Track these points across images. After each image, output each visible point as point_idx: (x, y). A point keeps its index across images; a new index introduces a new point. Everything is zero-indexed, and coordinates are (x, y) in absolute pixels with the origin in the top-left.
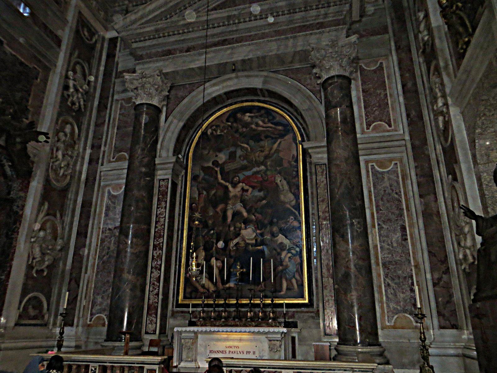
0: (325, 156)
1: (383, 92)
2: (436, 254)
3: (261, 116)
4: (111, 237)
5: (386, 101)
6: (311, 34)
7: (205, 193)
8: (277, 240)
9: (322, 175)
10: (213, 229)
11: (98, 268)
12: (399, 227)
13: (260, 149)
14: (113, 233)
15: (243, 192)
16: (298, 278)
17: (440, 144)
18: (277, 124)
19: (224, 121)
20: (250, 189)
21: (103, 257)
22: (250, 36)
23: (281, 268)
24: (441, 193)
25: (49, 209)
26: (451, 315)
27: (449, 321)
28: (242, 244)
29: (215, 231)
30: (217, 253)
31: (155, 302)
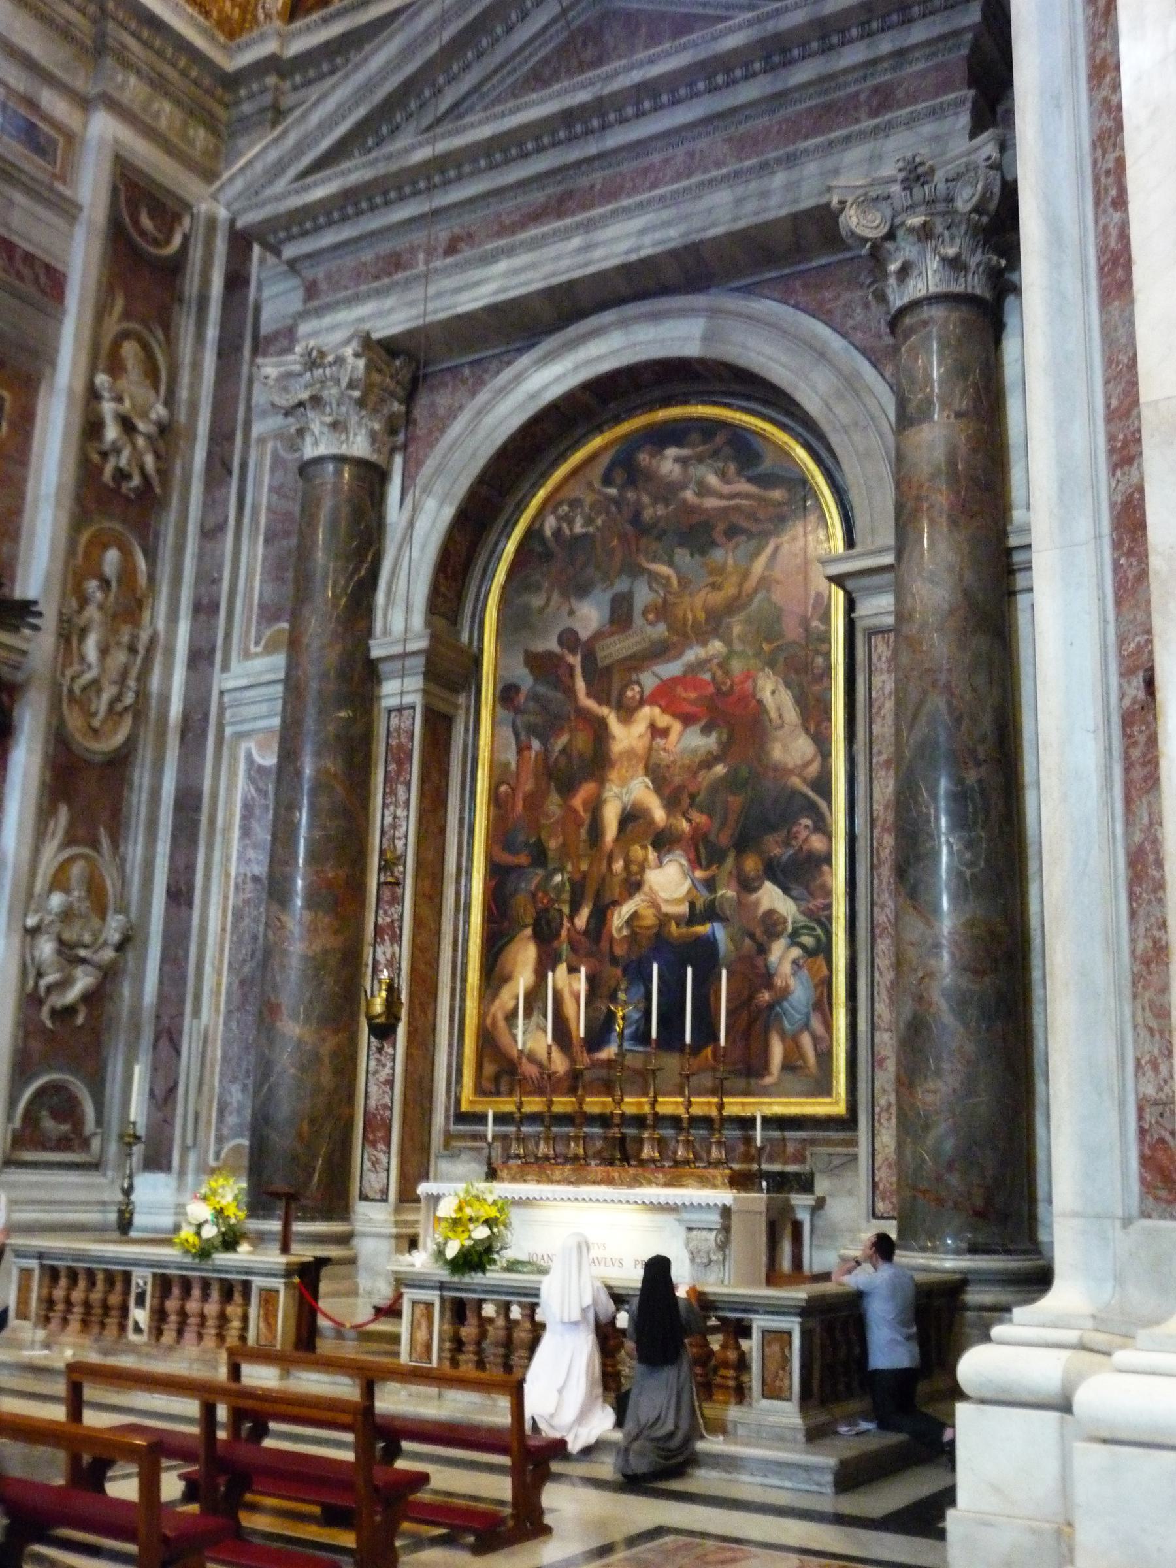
3: (715, 455)
6: (848, 139)
7: (536, 744)
8: (757, 904)
10: (561, 870)
11: (228, 1001)
13: (710, 580)
15: (653, 737)
18: (766, 481)
19: (597, 484)
20: (677, 727)
21: (241, 967)
22: (646, 171)
23: (766, 996)
25: (71, 824)
28: (649, 918)
29: (566, 876)
31: (385, 1107)
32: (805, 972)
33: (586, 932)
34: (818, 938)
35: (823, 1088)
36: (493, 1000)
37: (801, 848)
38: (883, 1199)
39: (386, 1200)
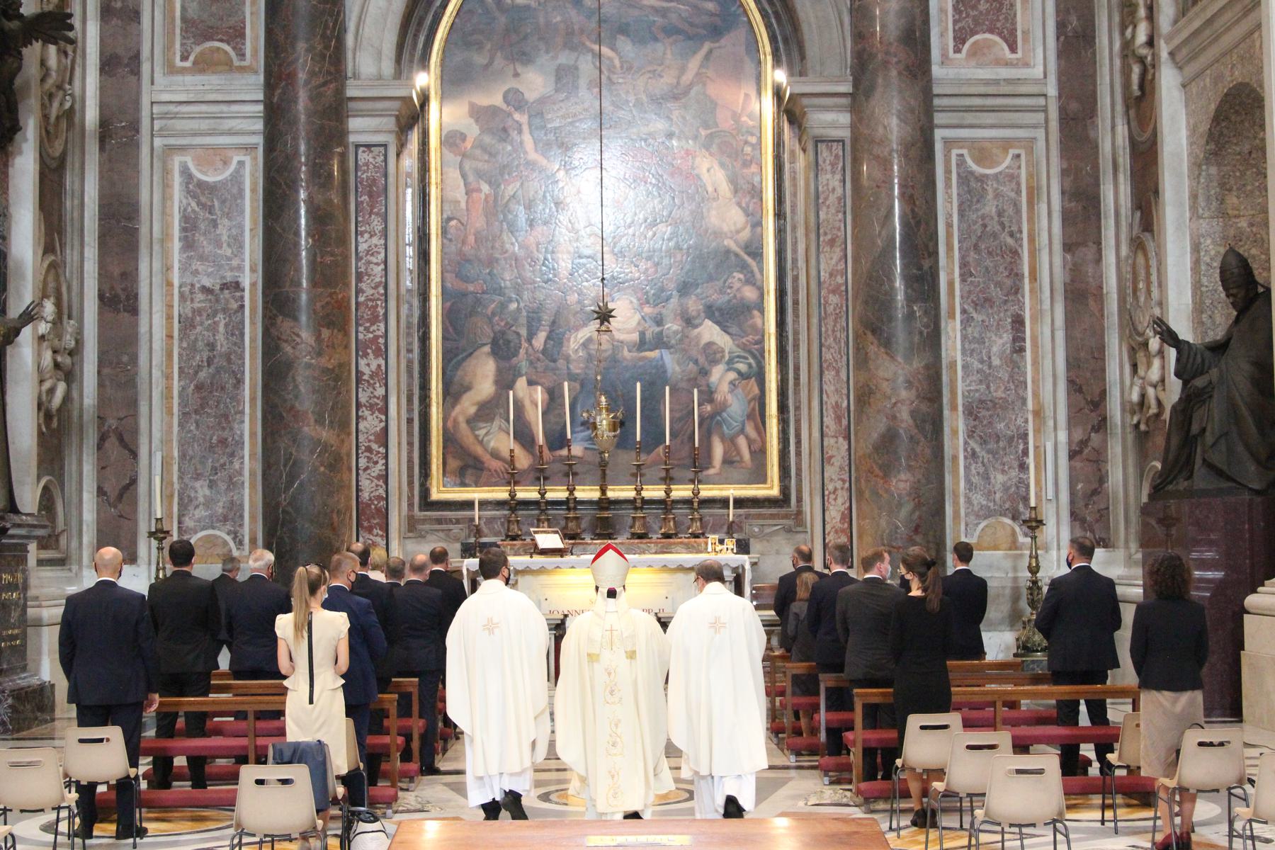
0: (845, 118)
2: (1084, 388)
4: (215, 313)
7: (485, 188)
8: (699, 337)
9: (833, 173)
11: (183, 403)
12: (1010, 320)
14: (217, 301)
16: (752, 433)
17: (1125, 122)
21: (196, 373)
23: (709, 408)
24: (1112, 242)
26: (1097, 521)
27: (1092, 531)
30: (531, 363)
31: (379, 498)
33: (544, 351)
34: (750, 366)
35: (759, 476)
36: (453, 407)
37: (735, 297)
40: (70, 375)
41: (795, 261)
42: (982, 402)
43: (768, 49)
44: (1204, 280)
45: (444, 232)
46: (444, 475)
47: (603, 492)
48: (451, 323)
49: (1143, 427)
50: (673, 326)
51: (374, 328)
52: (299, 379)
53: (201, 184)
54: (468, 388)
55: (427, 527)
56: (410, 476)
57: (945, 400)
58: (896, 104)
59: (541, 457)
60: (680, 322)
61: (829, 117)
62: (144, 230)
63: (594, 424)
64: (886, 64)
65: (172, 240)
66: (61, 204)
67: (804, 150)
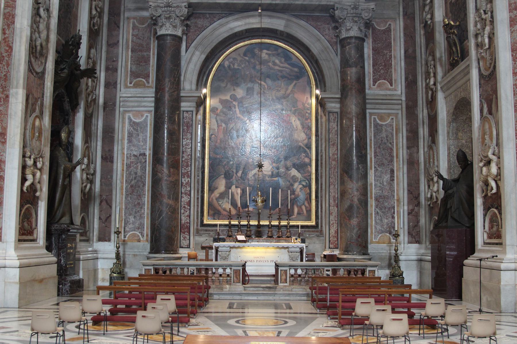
0: (338, 105)
1: (388, 53)
3: (278, 55)
5: (390, 62)
7: (224, 125)
9: (334, 123)
11: (126, 192)
16: (307, 205)
18: (293, 65)
19: (242, 55)
21: (131, 182)
23: (293, 196)
24: (422, 146)
26: (416, 235)
27: (415, 238)
30: (237, 181)
31: (187, 223)
32: (303, 191)
33: (241, 177)
34: (306, 183)
35: (309, 219)
36: (212, 194)
37: (302, 161)
38: (332, 244)
39: (189, 248)
40: (92, 182)
41: (321, 150)
42: (380, 196)
43: (314, 83)
44: (451, 159)
45: (210, 139)
46: (208, 216)
47: (259, 222)
48: (212, 168)
49: (431, 205)
50: (282, 170)
51: (187, 168)
52: (163, 184)
53: (134, 122)
54: (217, 188)
55: (202, 232)
56: (198, 216)
57: (369, 195)
58: (354, 101)
59: (239, 211)
60: (284, 169)
61: (333, 105)
62: (116, 136)
63: (257, 201)
64: (351, 89)
65: (125, 140)
66: (91, 128)
67: (325, 115)
